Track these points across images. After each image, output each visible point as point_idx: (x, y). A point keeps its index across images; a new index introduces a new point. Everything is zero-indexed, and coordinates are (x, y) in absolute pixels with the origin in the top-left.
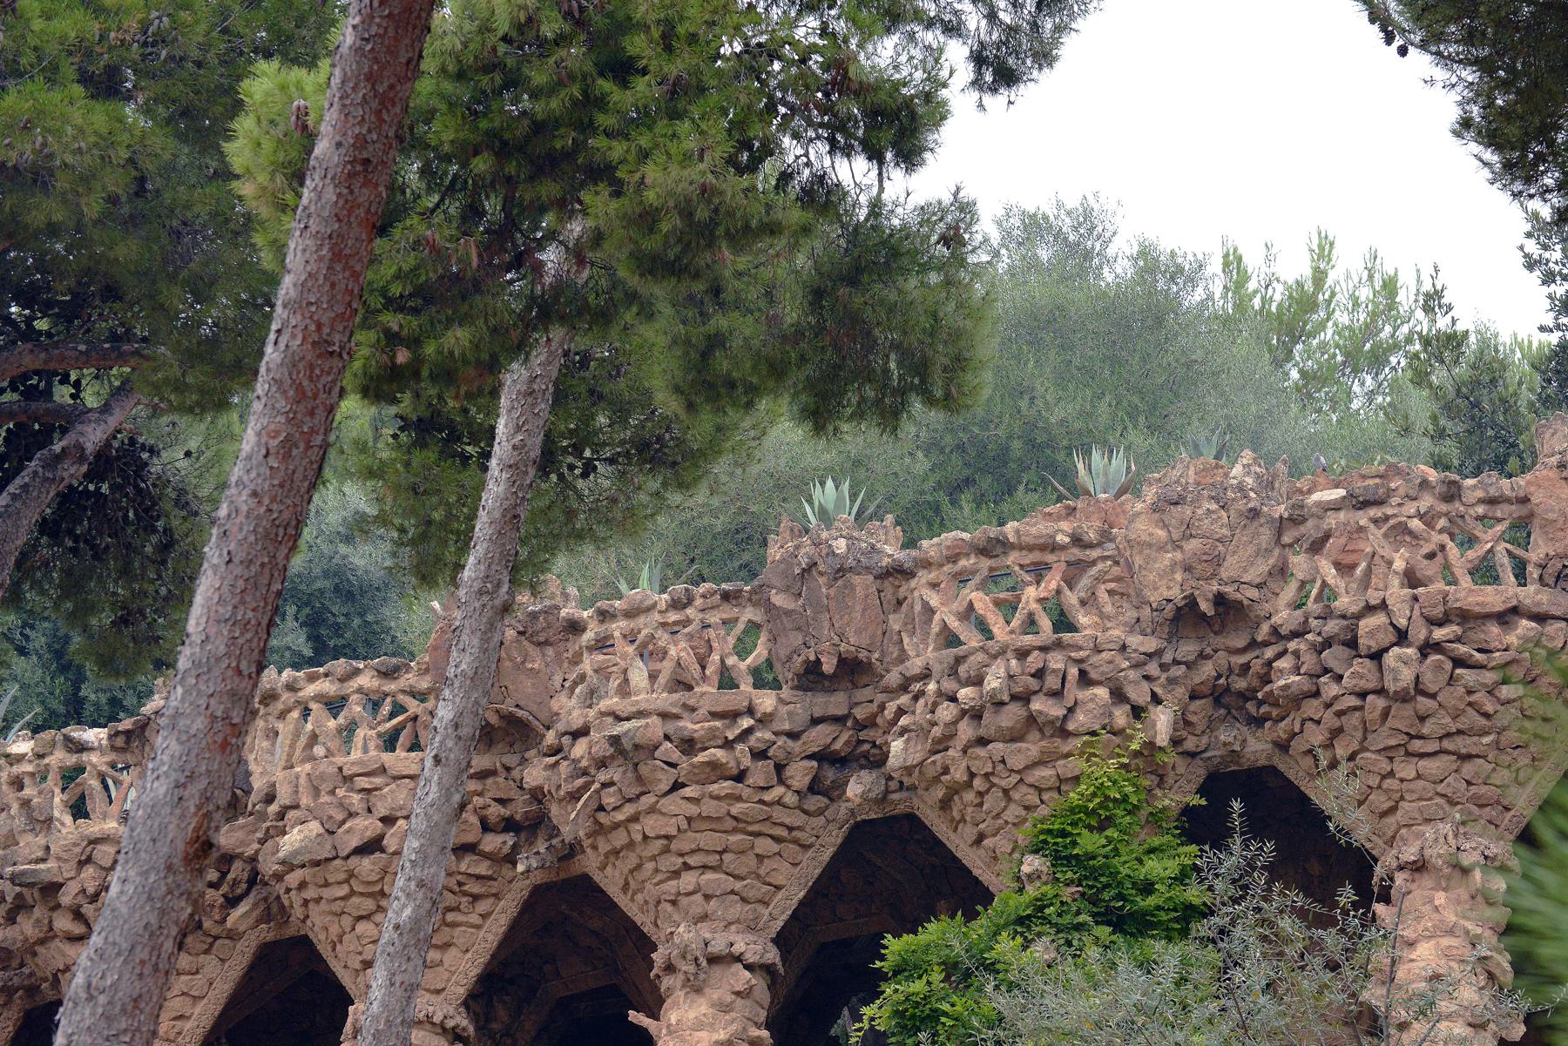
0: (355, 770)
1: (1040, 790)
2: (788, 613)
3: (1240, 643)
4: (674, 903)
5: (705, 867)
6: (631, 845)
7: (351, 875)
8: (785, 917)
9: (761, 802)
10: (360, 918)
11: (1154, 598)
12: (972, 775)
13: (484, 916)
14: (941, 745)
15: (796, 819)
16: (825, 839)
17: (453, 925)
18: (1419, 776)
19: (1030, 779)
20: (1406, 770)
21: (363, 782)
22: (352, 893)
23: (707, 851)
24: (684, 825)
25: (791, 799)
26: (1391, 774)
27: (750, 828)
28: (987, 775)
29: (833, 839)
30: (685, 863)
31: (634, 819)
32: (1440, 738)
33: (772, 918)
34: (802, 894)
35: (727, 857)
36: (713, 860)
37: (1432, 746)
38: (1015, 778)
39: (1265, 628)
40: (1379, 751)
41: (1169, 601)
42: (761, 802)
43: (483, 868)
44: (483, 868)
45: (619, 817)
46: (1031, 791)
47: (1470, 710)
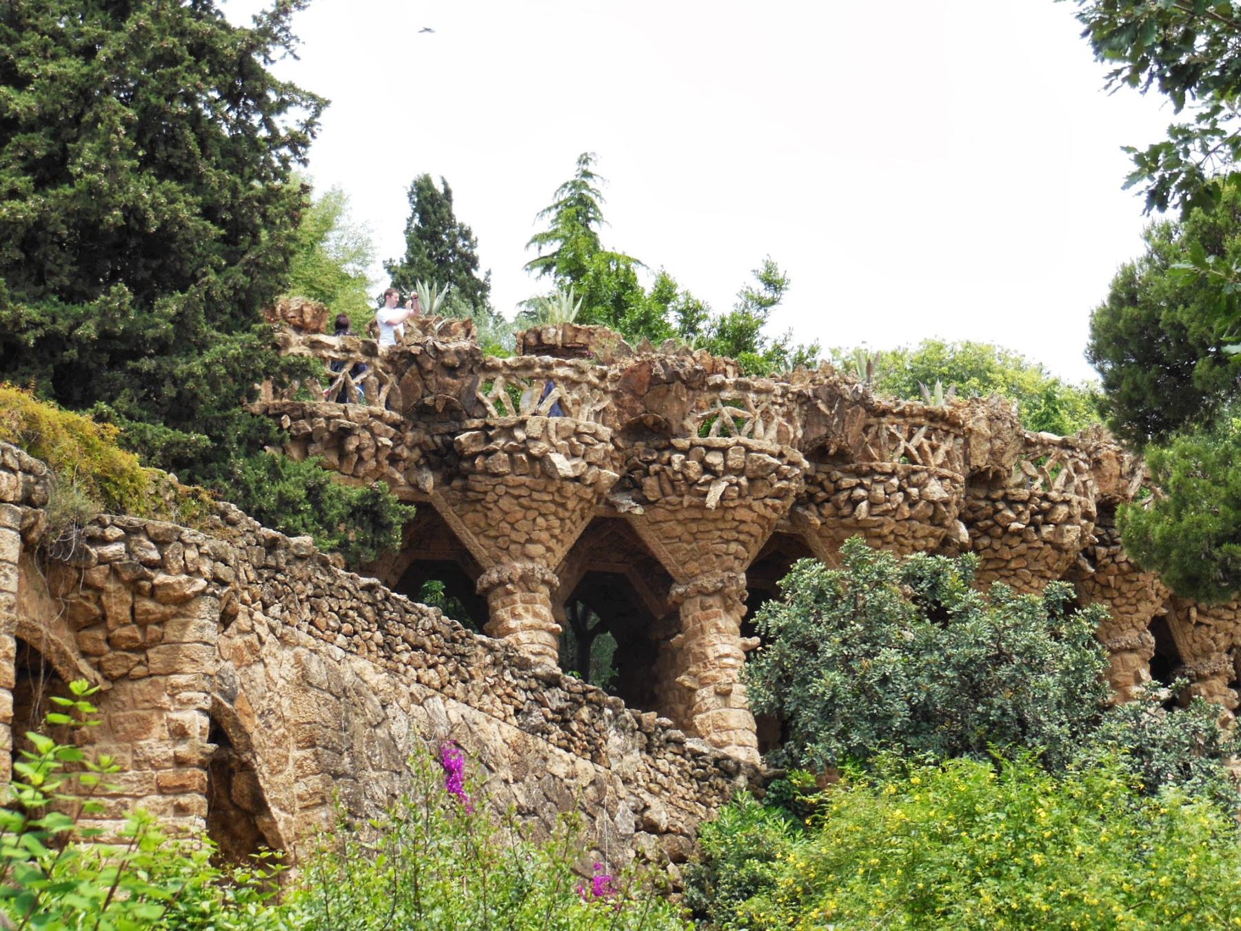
0: (585, 430)
2: (825, 415)
4: (717, 556)
5: (743, 544)
6: (715, 520)
7: (559, 490)
10: (540, 514)
12: (892, 532)
14: (885, 513)
21: (588, 439)
22: (553, 501)
28: (897, 535)
31: (734, 508)
39: (1001, 493)
45: (732, 505)
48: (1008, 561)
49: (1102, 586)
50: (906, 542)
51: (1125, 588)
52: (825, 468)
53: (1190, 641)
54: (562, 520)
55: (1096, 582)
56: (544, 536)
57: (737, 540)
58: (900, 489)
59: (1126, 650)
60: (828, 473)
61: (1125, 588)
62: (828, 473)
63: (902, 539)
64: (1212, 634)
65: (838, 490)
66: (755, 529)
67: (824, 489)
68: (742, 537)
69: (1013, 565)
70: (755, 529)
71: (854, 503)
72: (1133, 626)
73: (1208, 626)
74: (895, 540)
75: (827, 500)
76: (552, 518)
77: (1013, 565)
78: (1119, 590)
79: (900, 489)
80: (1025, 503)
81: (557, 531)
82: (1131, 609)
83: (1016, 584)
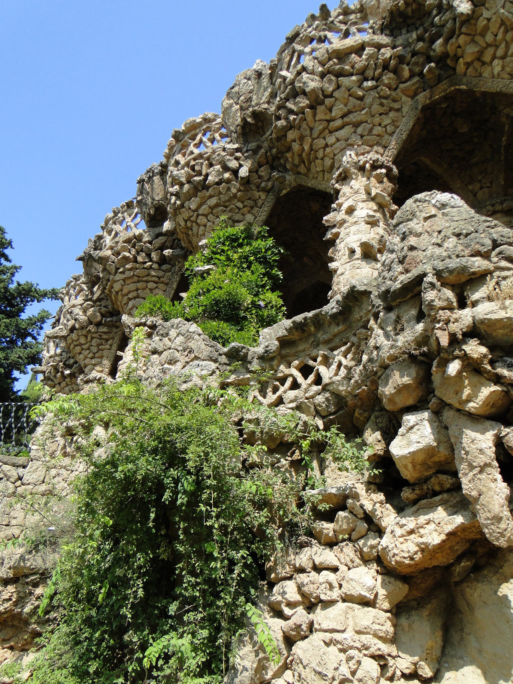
1: (206, 216)
5: (135, 298)
9: (144, 268)
13: (111, 345)
15: (161, 273)
16: (173, 280)
17: (103, 350)
18: (338, 140)
19: (200, 212)
20: (331, 140)
23: (133, 291)
24: (122, 282)
25: (155, 266)
26: (327, 146)
27: (144, 279)
30: (129, 298)
32: (342, 117)
35: (139, 292)
36: (134, 294)
37: (339, 123)
40: (318, 137)
43: (105, 329)
44: (105, 329)
46: (203, 217)
47: (351, 98)
54: (89, 349)
55: (472, 62)
56: (87, 361)
57: (130, 299)
61: (489, 38)
66: (132, 287)
68: (130, 296)
70: (132, 287)
76: (83, 352)
78: (489, 45)
81: (91, 355)
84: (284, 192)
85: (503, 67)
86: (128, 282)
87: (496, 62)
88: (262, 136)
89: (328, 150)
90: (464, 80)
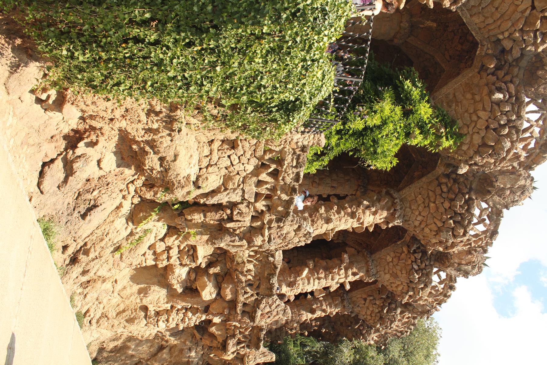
3: (473, 186)
8: (460, 13)
11: (500, 177)
12: (479, 117)
19: (468, 136)
20: (419, 218)
25: (501, 37)
26: (420, 214)
28: (476, 122)
29: (478, 38)
33: (462, 10)
34: (465, 21)
37: (422, 226)
38: (471, 133)
40: (427, 216)
41: (497, 181)
42: (508, 30)
48: (434, 202)
49: (399, 257)
50: (470, 129)
51: (398, 268)
52: (521, 76)
53: (358, 296)
58: (509, 121)
59: (368, 268)
60: (517, 76)
62: (517, 76)
63: (473, 125)
64: (361, 306)
65: (505, 83)
67: (506, 74)
69: (432, 205)
71: (500, 90)
72: (378, 272)
73: (364, 304)
74: (472, 121)
75: (498, 79)
77: (432, 205)
78: (397, 265)
79: (509, 121)
80: (469, 210)
82: (386, 271)
83: (420, 208)
84: (439, 162)
85: (386, 260)
86: (511, 9)
87: (390, 260)
88: (480, 179)
89: (417, 213)
90: (400, 246)
